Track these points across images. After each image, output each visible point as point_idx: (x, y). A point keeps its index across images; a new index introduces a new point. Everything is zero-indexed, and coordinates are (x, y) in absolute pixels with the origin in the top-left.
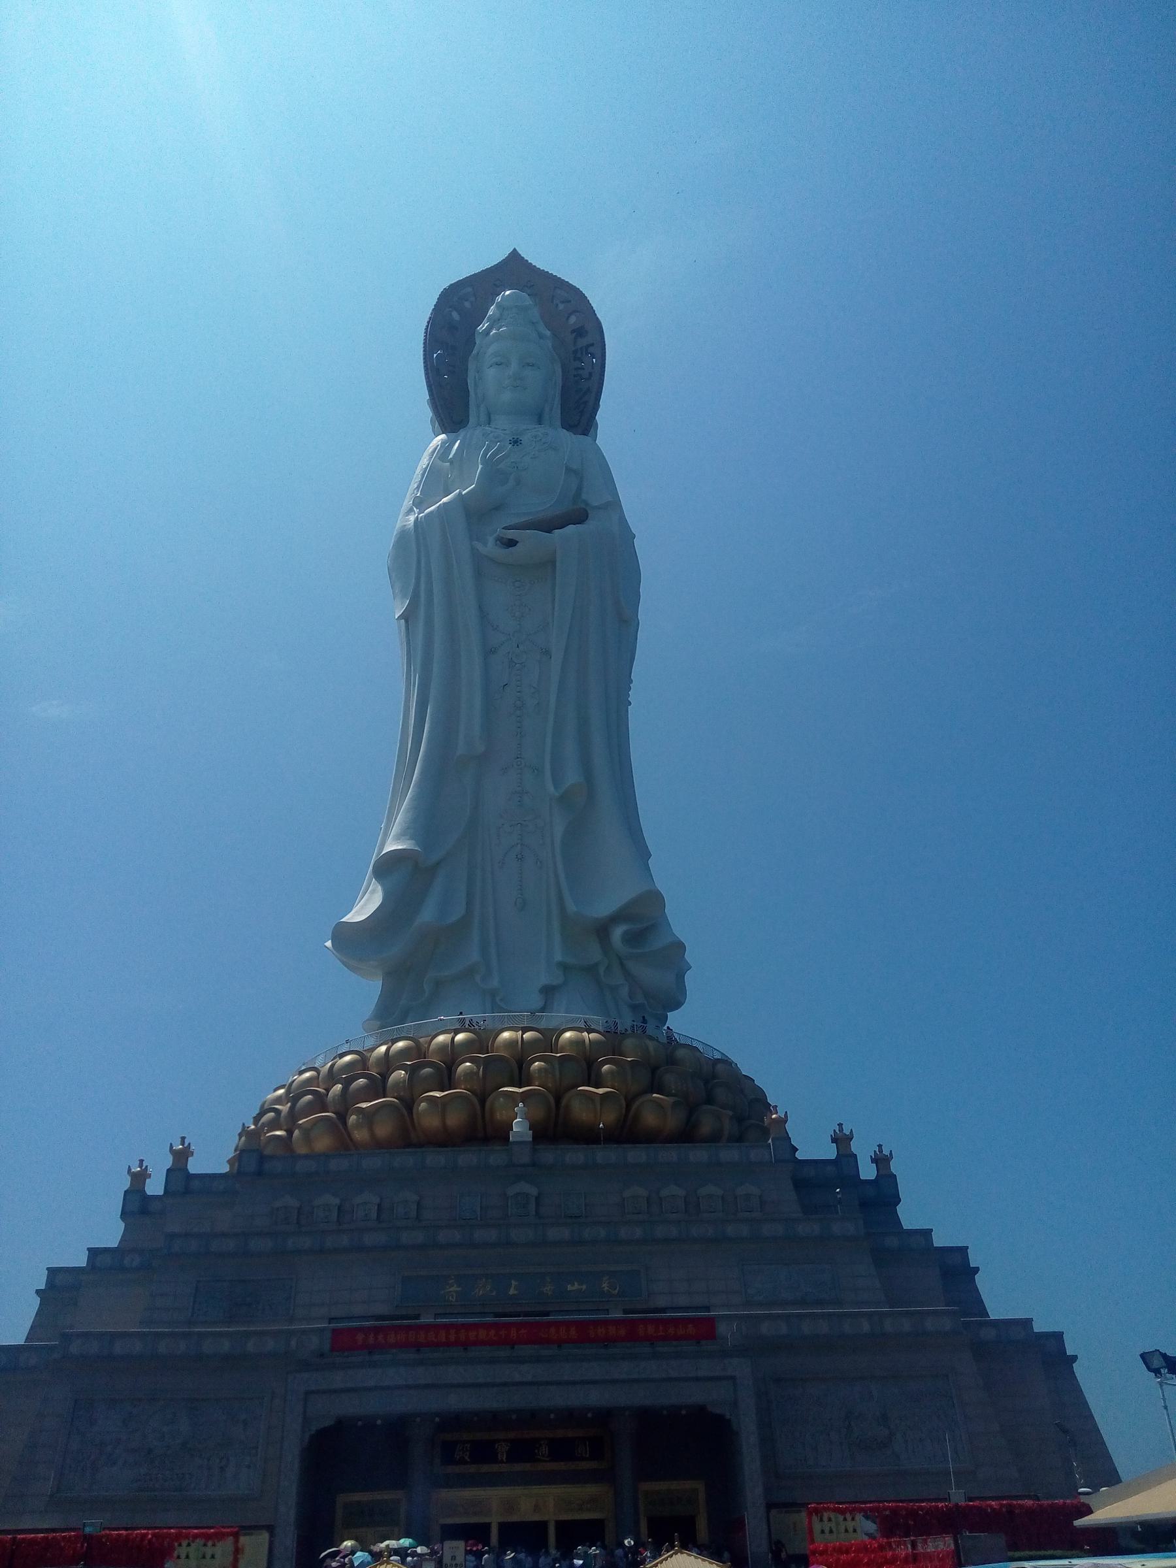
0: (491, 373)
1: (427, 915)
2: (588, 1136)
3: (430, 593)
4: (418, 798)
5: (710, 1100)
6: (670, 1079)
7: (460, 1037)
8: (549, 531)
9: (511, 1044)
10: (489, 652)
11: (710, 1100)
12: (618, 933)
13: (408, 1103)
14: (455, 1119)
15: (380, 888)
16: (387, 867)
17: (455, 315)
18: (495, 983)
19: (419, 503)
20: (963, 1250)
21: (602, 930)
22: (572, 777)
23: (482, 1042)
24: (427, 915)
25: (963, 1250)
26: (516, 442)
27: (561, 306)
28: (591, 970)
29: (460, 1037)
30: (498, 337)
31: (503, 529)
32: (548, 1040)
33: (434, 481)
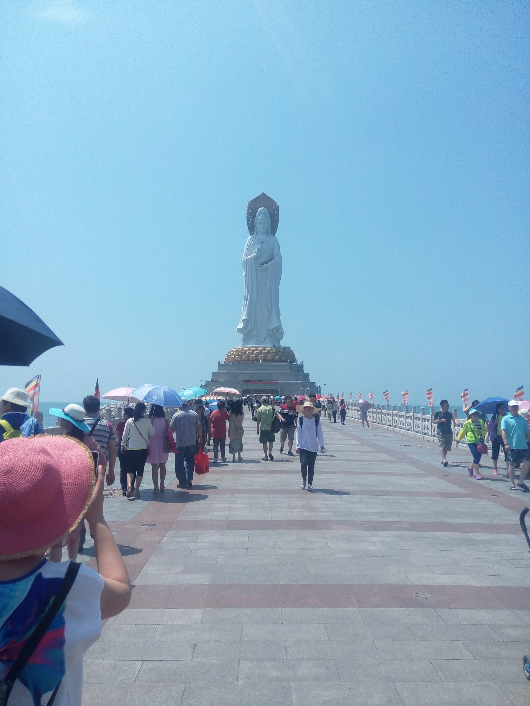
0: (258, 225)
1: (249, 328)
2: (268, 361)
3: (249, 273)
4: (247, 310)
5: (283, 355)
6: (278, 354)
7: (254, 349)
8: (267, 263)
9: (260, 350)
10: (257, 284)
11: (283, 355)
12: (274, 331)
13: (249, 356)
14: (254, 359)
15: (243, 323)
16: (243, 321)
17: (252, 207)
18: (258, 337)
19: (246, 255)
20: (308, 373)
21: (273, 329)
22: (269, 307)
23: (257, 350)
24: (249, 328)
25: (308, 373)
26: (262, 242)
27: (272, 204)
29: (254, 349)
30: (260, 218)
31: (260, 264)
32: (264, 350)
33: (249, 249)
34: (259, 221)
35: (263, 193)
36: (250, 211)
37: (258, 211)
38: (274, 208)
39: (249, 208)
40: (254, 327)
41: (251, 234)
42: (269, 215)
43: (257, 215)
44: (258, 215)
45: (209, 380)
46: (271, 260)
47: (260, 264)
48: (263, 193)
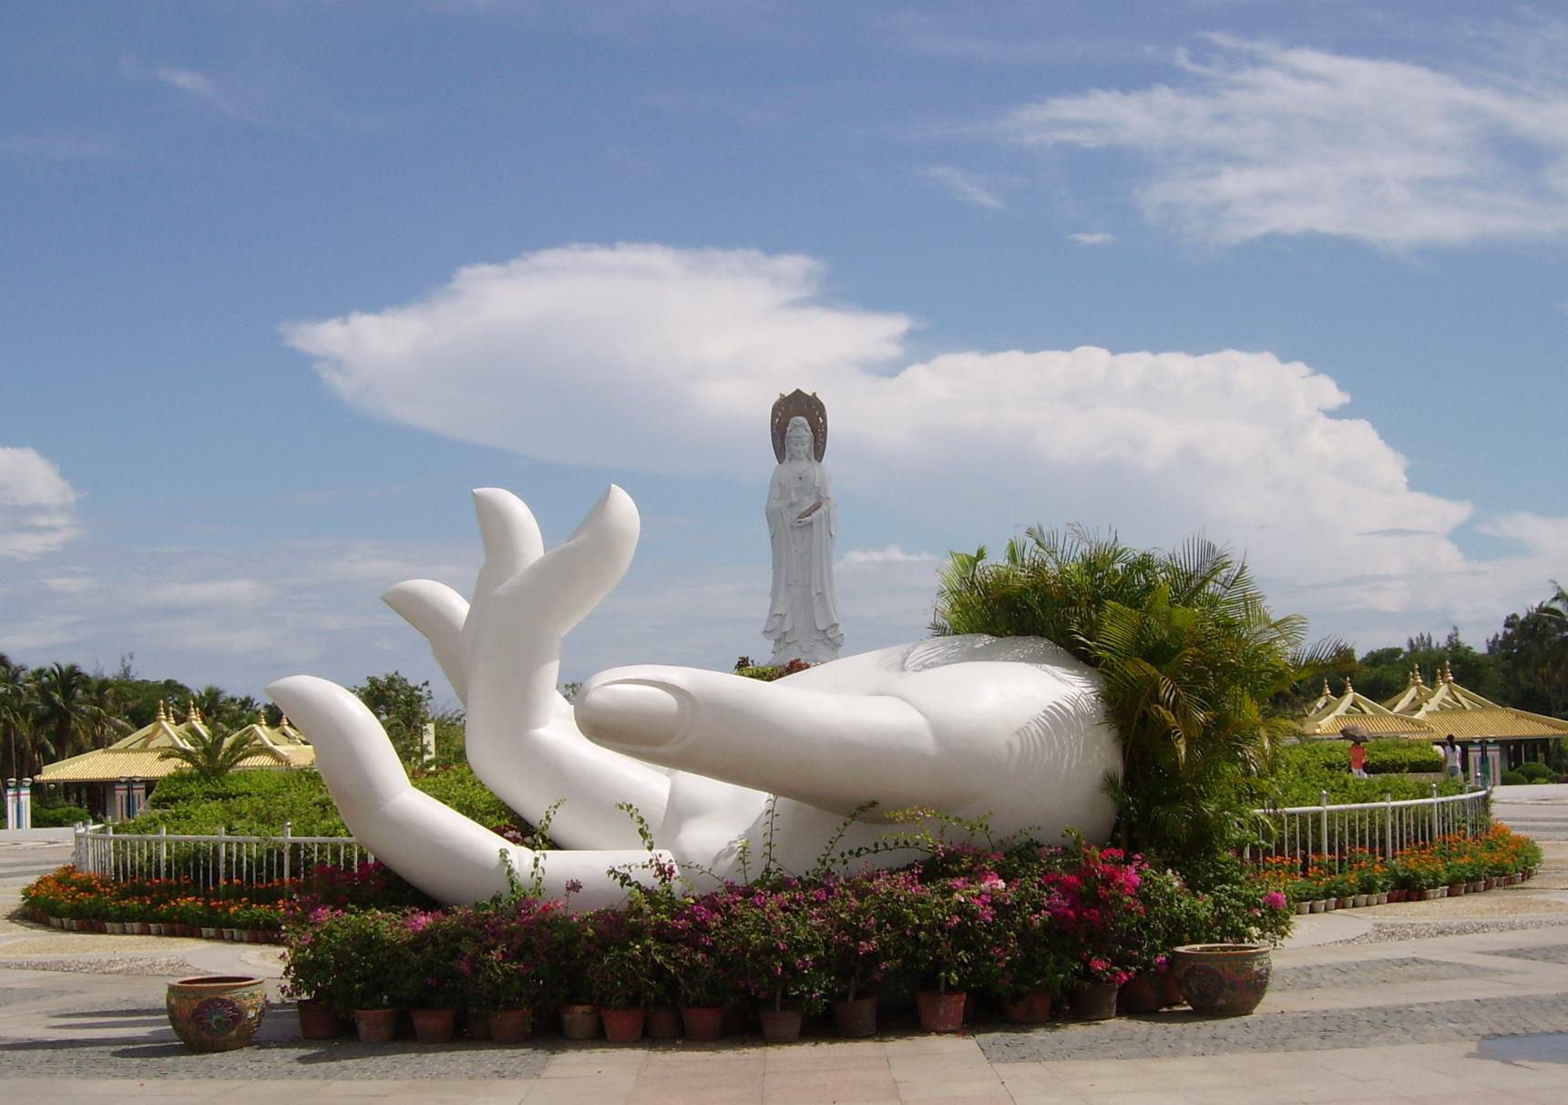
8: (809, 515)
10: (796, 551)
12: (828, 631)
21: (825, 631)
28: (822, 640)
31: (799, 518)
34: (793, 439)
35: (798, 390)
37: (790, 424)
38: (817, 413)
40: (793, 629)
41: (780, 463)
42: (809, 428)
43: (788, 429)
44: (791, 430)
46: (819, 507)
47: (799, 518)
48: (798, 390)
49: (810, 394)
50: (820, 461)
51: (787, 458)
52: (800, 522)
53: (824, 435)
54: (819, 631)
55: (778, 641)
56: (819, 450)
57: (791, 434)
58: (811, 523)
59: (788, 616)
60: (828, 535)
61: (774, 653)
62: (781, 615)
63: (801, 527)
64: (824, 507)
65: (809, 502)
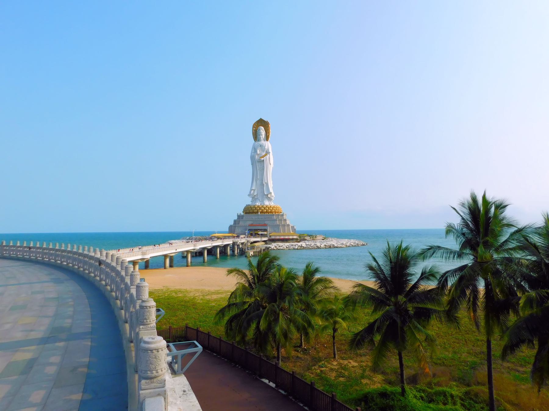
35: (261, 118)
36: (254, 129)
39: (253, 127)
40: (257, 194)
43: (257, 130)
45: (232, 223)
48: (261, 118)
49: (266, 121)
50: (268, 141)
51: (257, 140)
52: (260, 160)
53: (269, 133)
54: (266, 195)
55: (253, 198)
56: (267, 138)
57: (259, 132)
58: (264, 160)
59: (256, 191)
60: (269, 164)
61: (251, 202)
62: (253, 189)
63: (260, 161)
64: (268, 155)
65: (264, 154)
